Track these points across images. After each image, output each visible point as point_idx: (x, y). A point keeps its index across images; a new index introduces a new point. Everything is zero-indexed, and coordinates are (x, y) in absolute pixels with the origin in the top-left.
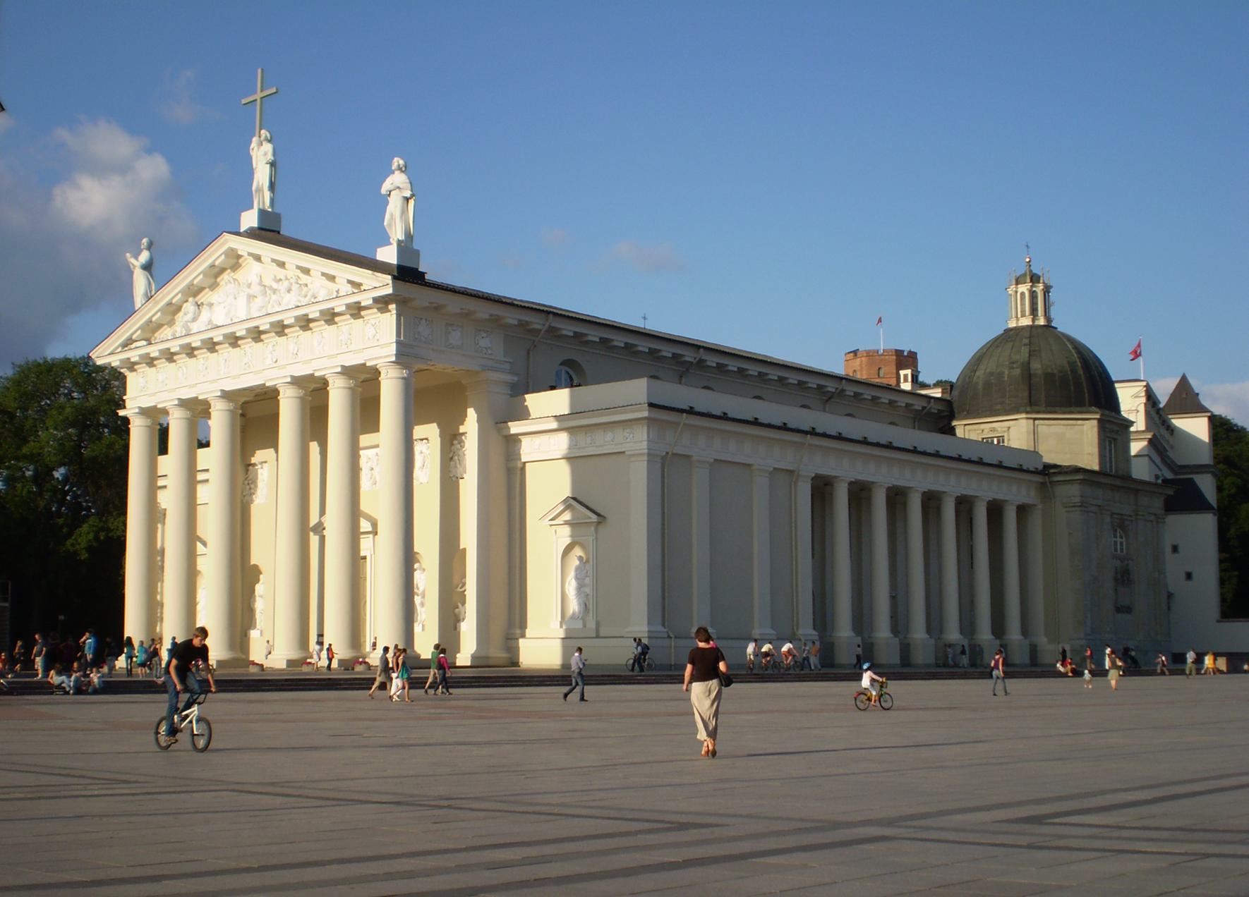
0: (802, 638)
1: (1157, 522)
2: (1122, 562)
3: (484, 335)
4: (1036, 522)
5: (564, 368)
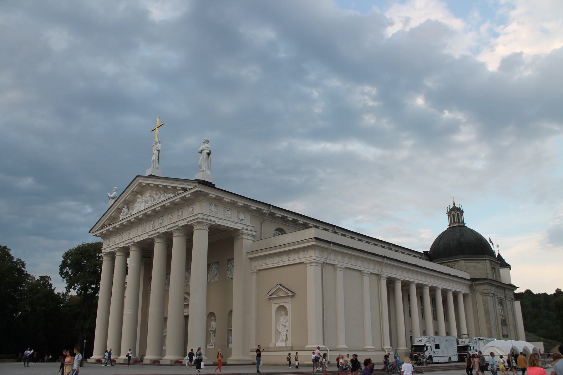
0: (386, 350)
1: (512, 301)
2: (503, 317)
3: (242, 214)
4: (470, 300)
5: (277, 231)
